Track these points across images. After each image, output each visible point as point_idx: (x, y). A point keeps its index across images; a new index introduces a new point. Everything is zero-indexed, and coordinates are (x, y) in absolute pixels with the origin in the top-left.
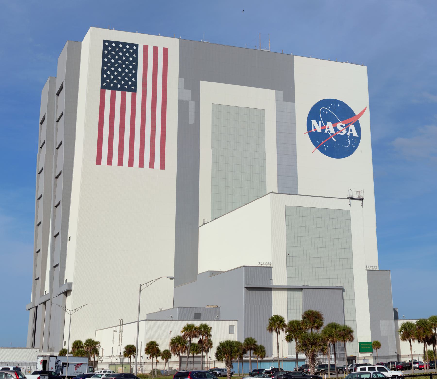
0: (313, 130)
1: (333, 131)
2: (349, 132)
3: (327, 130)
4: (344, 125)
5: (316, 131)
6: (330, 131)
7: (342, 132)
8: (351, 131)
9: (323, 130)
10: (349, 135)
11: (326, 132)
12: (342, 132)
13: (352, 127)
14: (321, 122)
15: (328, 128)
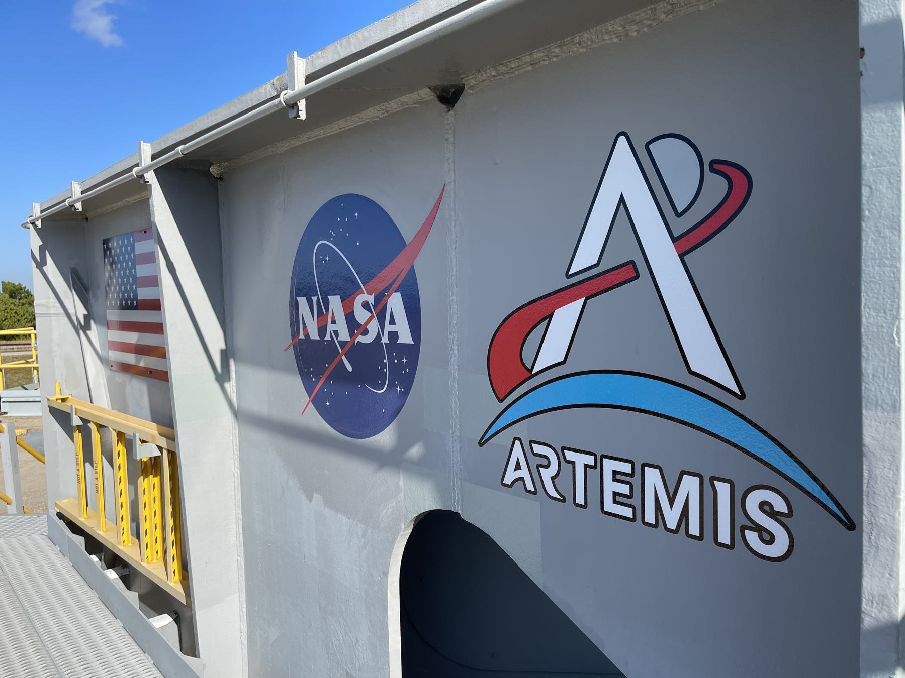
0: (302, 337)
1: (344, 336)
2: (388, 328)
3: (330, 328)
4: (371, 299)
5: (307, 335)
6: (336, 333)
7: (365, 332)
8: (392, 322)
9: (322, 330)
10: (385, 340)
11: (328, 338)
12: (365, 332)
13: (395, 302)
14: (318, 301)
15: (334, 322)
